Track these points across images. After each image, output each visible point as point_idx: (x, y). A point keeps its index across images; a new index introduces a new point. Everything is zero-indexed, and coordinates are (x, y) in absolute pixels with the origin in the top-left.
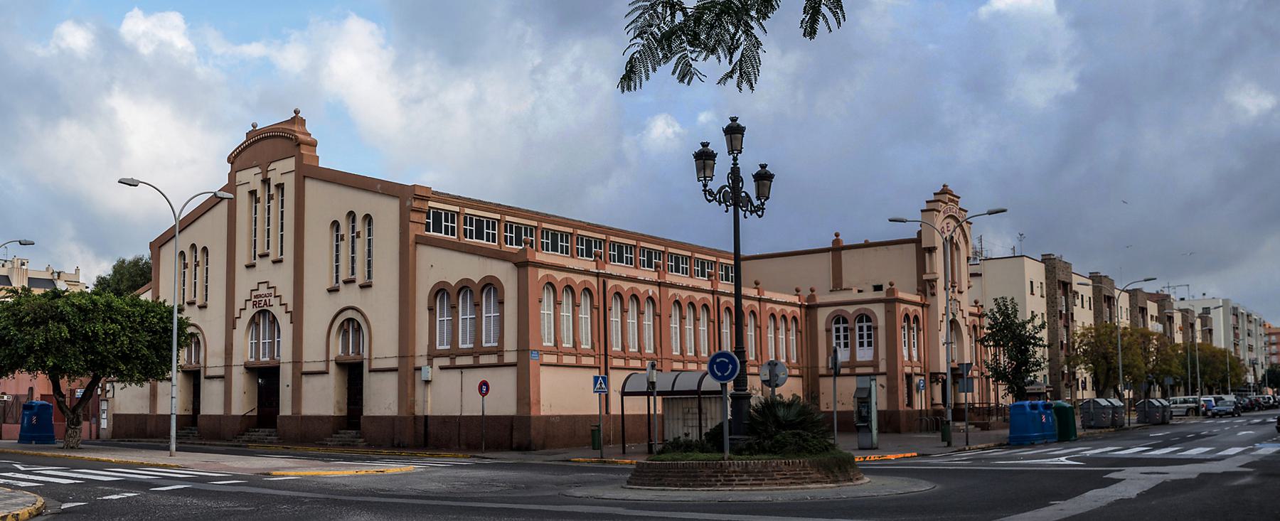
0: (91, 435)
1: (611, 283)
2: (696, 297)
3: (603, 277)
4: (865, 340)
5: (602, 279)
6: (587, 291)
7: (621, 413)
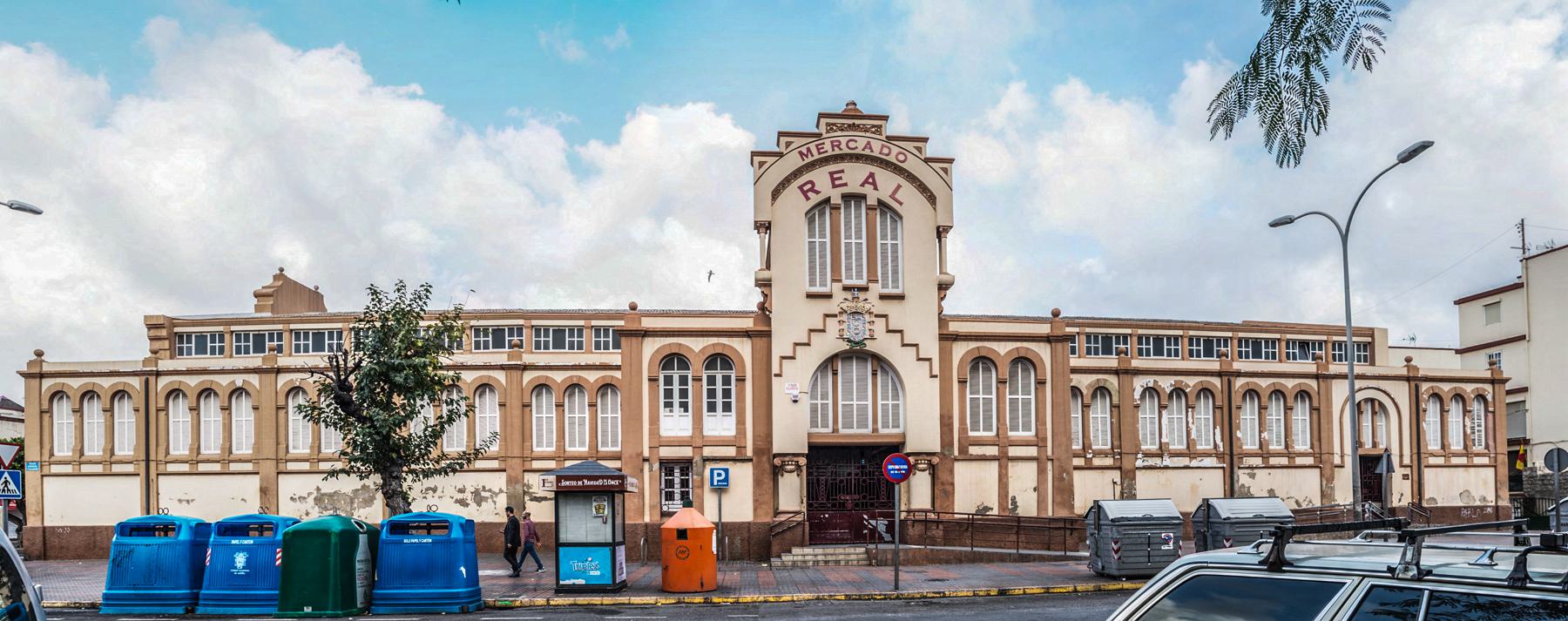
0: (803, 539)
1: (1239, 383)
2: (555, 378)
3: (1227, 375)
4: (719, 400)
5: (1227, 378)
6: (1206, 391)
7: (554, 521)
